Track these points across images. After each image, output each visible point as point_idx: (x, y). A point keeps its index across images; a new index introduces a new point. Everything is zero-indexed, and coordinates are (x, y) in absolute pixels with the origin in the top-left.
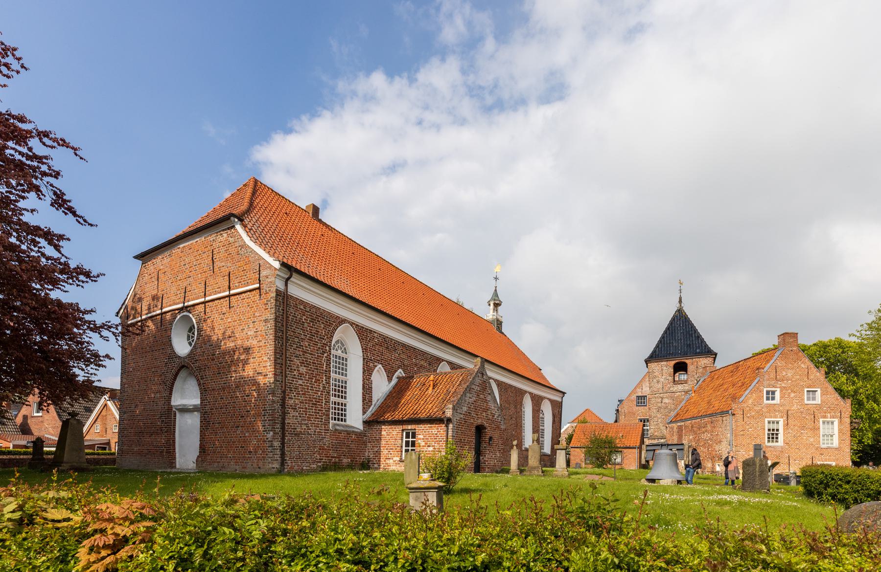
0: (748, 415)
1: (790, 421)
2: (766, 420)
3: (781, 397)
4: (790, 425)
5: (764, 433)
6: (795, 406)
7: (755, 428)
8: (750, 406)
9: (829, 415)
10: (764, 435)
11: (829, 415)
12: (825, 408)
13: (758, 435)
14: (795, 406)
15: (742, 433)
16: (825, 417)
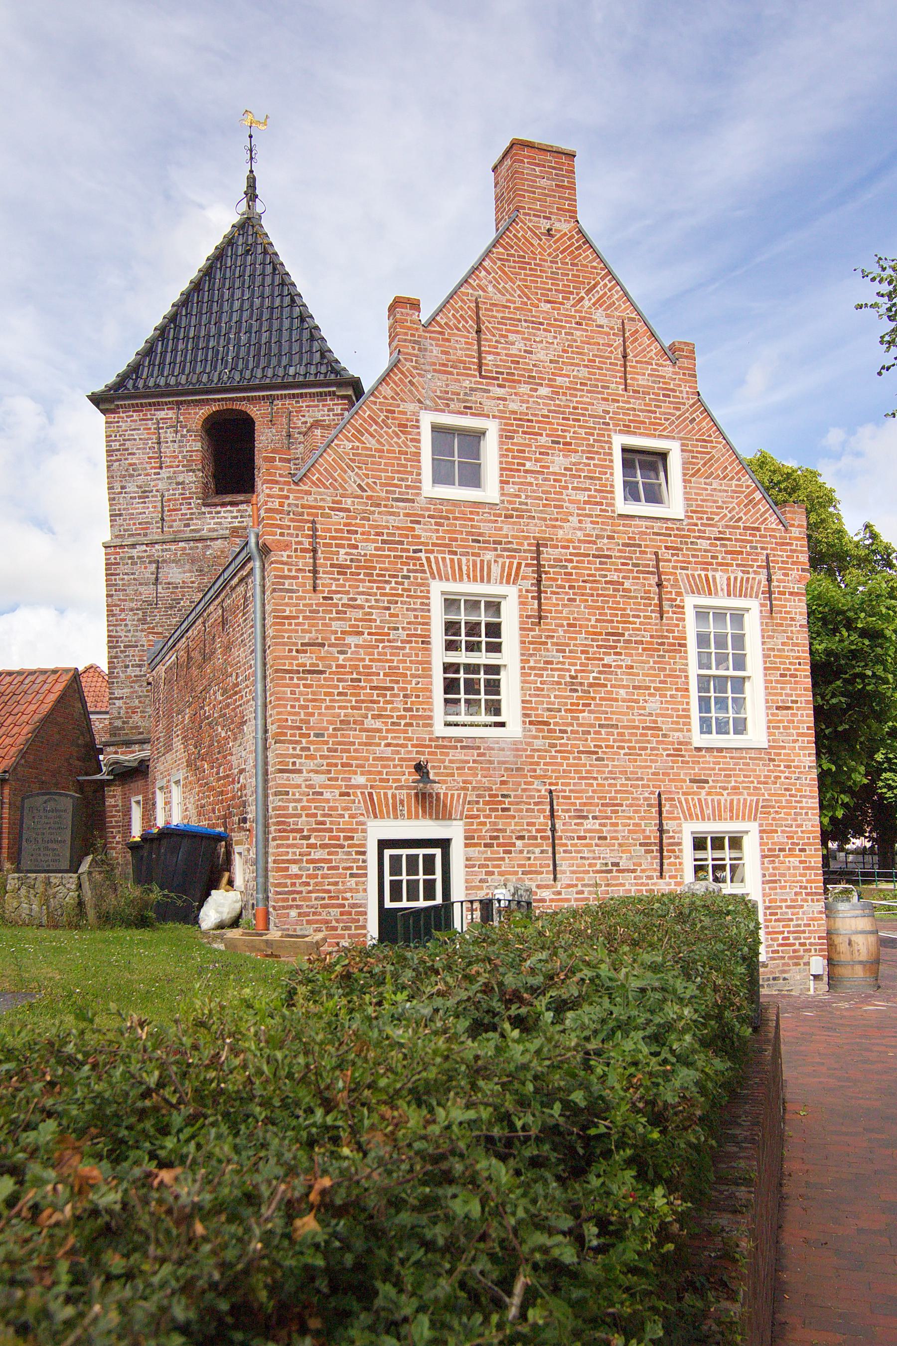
0: (342, 556)
1: (550, 601)
2: (437, 589)
3: (507, 471)
4: (550, 622)
5: (426, 665)
6: (574, 520)
7: (380, 634)
8: (348, 502)
9: (720, 577)
10: (427, 673)
11: (720, 577)
12: (704, 544)
13: (392, 673)
14: (574, 520)
15: (306, 659)
16: (709, 589)
